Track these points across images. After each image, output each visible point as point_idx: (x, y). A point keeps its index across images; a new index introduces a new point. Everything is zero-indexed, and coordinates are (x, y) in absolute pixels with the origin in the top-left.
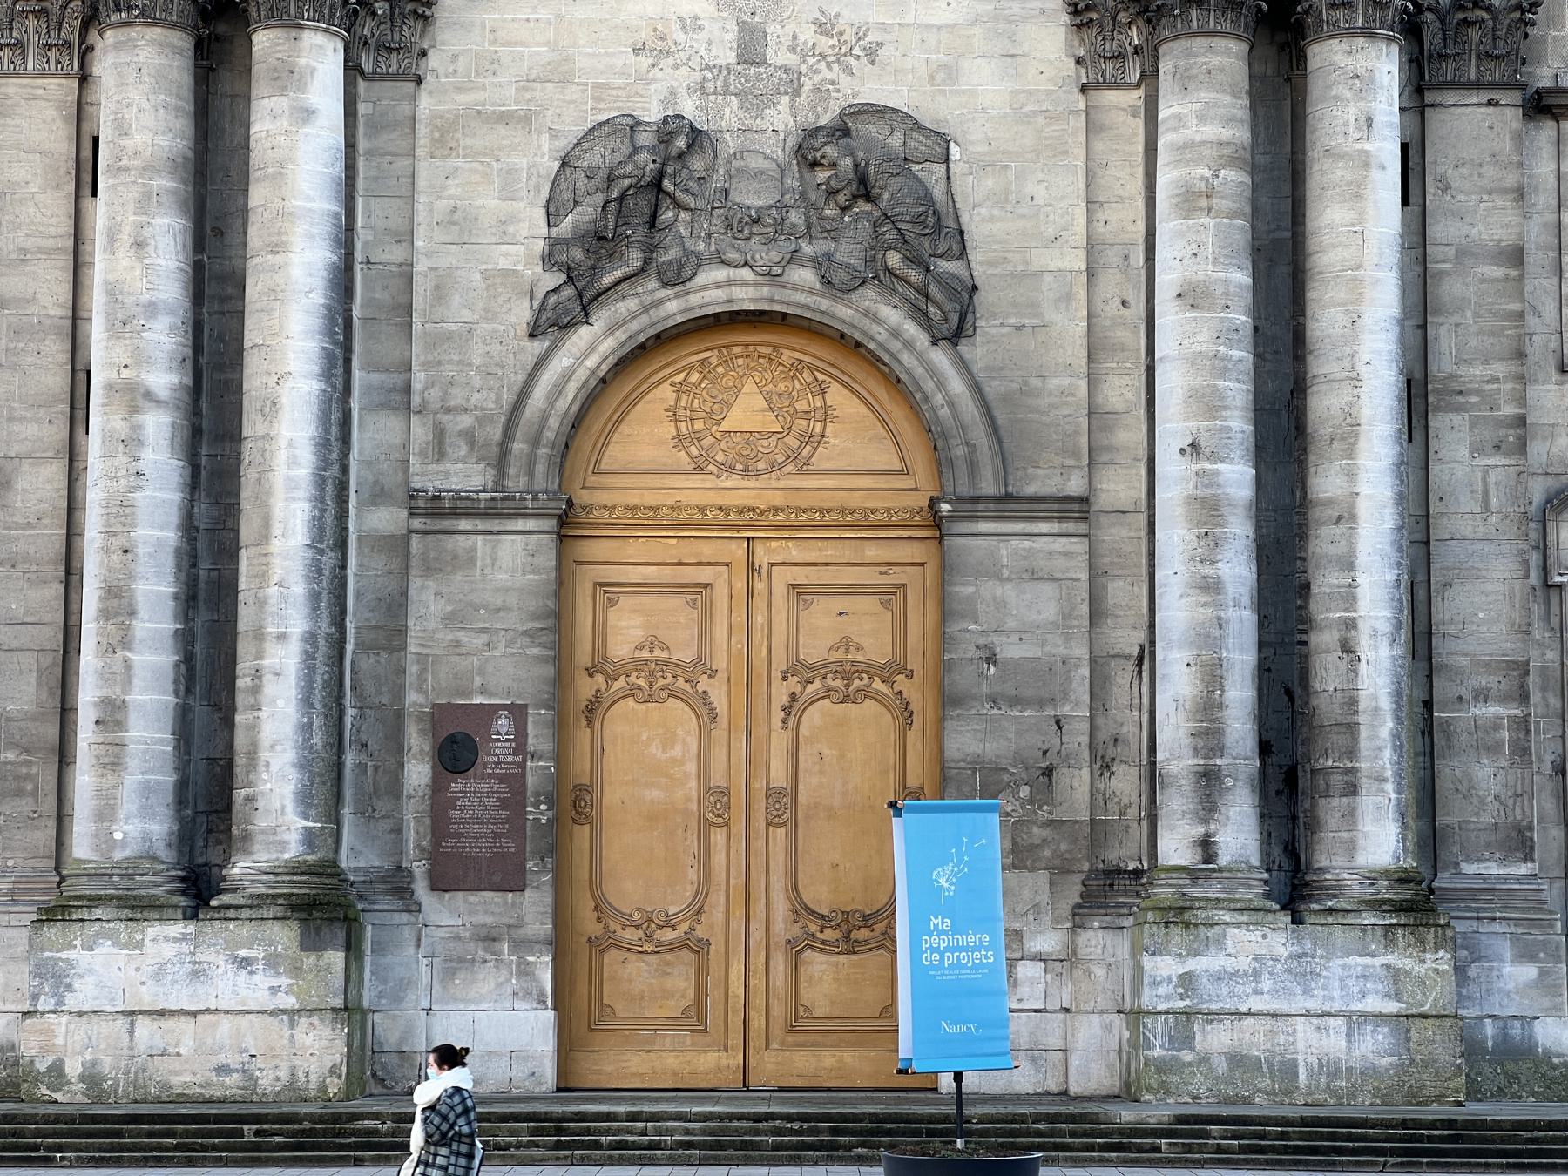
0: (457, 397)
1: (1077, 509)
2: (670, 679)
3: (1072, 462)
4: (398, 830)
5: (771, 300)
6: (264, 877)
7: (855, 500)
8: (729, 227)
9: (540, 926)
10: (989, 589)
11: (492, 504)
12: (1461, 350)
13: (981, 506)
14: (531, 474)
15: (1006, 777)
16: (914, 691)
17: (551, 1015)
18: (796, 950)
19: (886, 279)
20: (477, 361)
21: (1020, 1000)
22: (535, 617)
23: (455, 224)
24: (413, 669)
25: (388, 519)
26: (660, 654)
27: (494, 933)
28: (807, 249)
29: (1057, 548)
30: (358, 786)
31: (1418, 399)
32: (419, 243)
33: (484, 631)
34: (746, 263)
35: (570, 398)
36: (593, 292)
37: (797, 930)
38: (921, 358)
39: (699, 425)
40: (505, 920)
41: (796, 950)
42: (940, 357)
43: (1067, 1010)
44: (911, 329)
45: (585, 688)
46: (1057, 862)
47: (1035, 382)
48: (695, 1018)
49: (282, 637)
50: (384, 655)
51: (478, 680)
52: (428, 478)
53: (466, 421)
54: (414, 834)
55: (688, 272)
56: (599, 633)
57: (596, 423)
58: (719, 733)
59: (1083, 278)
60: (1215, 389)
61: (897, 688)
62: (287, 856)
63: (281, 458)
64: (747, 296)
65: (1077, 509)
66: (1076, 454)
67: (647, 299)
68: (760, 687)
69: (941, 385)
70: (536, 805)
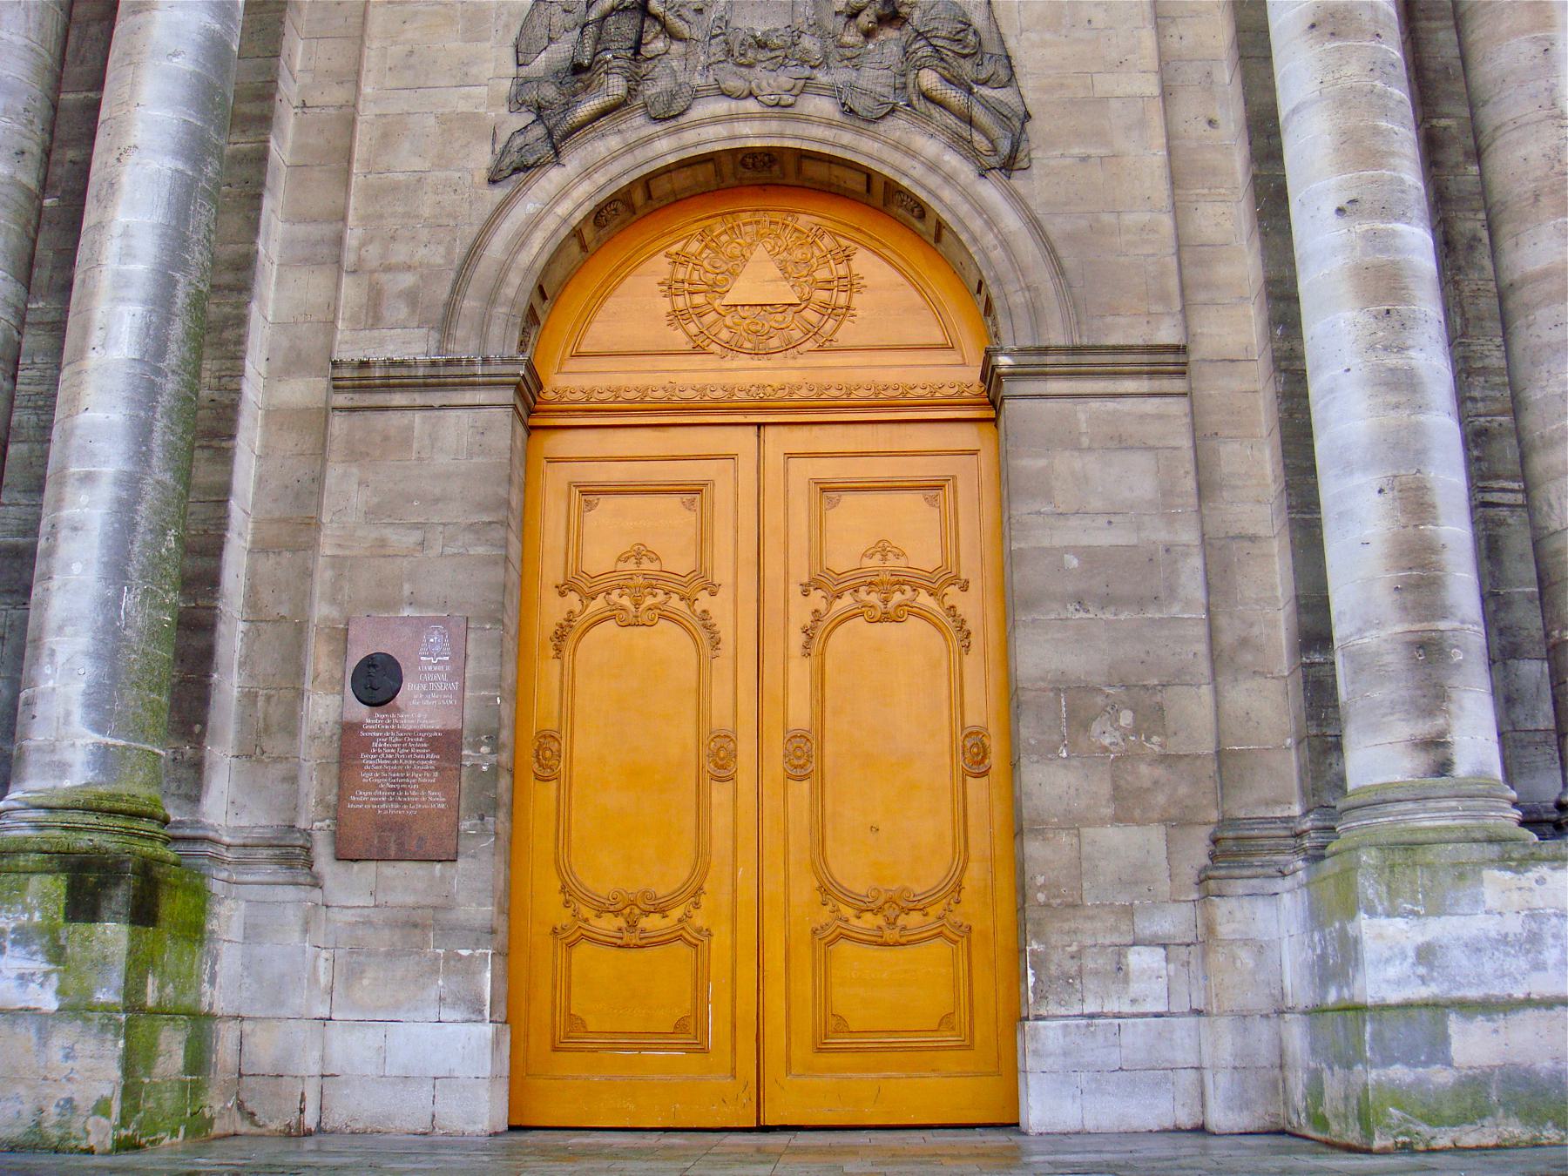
0: (400, 253)
1: (1171, 362)
2: (661, 597)
3: (1158, 308)
4: (292, 779)
5: (782, 136)
6: (32, 814)
7: (890, 377)
8: (729, 53)
9: (478, 910)
10: (1065, 463)
11: (433, 371)
13: (1050, 359)
14: (483, 337)
15: (1100, 700)
16: (969, 605)
17: (488, 1029)
18: (828, 939)
20: (426, 211)
21: (1133, 1001)
22: (482, 507)
23: (410, 67)
24: (323, 576)
25: (305, 390)
26: (646, 565)
27: (417, 916)
28: (821, 77)
30: (243, 720)
32: (367, 89)
33: (416, 526)
34: (751, 94)
35: (535, 250)
36: (565, 127)
37: (825, 915)
38: (966, 194)
39: (699, 299)
40: (430, 901)
41: (828, 939)
42: (990, 191)
43: (1199, 1012)
44: (952, 161)
45: (553, 609)
46: (1174, 812)
47: (1107, 218)
48: (688, 1034)
49: (88, 479)
50: (288, 555)
51: (407, 588)
53: (407, 280)
54: (313, 787)
55: (678, 105)
56: (574, 540)
57: (574, 301)
58: (723, 663)
59: (1158, 103)
60: (1376, 131)
61: (948, 602)
62: (67, 783)
63: (111, 249)
64: (754, 134)
66: (1164, 298)
67: (632, 137)
68: (773, 602)
69: (991, 223)
70: (476, 746)
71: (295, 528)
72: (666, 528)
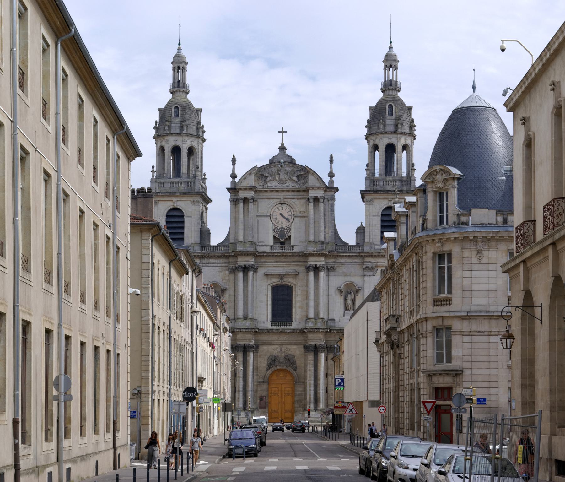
1: (304, 382)
12: (330, 372)
19: (291, 367)
25: (256, 383)
29: (303, 385)
31: (327, 375)
52: (259, 380)
54: (258, 405)
64: (281, 368)
65: (304, 382)
71: (256, 391)
72: (277, 389)
